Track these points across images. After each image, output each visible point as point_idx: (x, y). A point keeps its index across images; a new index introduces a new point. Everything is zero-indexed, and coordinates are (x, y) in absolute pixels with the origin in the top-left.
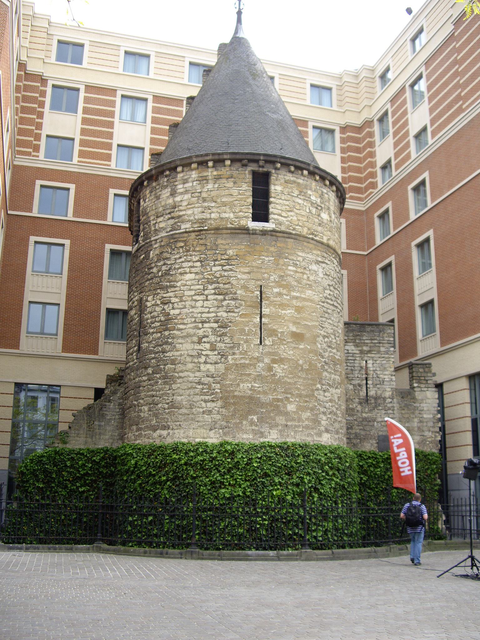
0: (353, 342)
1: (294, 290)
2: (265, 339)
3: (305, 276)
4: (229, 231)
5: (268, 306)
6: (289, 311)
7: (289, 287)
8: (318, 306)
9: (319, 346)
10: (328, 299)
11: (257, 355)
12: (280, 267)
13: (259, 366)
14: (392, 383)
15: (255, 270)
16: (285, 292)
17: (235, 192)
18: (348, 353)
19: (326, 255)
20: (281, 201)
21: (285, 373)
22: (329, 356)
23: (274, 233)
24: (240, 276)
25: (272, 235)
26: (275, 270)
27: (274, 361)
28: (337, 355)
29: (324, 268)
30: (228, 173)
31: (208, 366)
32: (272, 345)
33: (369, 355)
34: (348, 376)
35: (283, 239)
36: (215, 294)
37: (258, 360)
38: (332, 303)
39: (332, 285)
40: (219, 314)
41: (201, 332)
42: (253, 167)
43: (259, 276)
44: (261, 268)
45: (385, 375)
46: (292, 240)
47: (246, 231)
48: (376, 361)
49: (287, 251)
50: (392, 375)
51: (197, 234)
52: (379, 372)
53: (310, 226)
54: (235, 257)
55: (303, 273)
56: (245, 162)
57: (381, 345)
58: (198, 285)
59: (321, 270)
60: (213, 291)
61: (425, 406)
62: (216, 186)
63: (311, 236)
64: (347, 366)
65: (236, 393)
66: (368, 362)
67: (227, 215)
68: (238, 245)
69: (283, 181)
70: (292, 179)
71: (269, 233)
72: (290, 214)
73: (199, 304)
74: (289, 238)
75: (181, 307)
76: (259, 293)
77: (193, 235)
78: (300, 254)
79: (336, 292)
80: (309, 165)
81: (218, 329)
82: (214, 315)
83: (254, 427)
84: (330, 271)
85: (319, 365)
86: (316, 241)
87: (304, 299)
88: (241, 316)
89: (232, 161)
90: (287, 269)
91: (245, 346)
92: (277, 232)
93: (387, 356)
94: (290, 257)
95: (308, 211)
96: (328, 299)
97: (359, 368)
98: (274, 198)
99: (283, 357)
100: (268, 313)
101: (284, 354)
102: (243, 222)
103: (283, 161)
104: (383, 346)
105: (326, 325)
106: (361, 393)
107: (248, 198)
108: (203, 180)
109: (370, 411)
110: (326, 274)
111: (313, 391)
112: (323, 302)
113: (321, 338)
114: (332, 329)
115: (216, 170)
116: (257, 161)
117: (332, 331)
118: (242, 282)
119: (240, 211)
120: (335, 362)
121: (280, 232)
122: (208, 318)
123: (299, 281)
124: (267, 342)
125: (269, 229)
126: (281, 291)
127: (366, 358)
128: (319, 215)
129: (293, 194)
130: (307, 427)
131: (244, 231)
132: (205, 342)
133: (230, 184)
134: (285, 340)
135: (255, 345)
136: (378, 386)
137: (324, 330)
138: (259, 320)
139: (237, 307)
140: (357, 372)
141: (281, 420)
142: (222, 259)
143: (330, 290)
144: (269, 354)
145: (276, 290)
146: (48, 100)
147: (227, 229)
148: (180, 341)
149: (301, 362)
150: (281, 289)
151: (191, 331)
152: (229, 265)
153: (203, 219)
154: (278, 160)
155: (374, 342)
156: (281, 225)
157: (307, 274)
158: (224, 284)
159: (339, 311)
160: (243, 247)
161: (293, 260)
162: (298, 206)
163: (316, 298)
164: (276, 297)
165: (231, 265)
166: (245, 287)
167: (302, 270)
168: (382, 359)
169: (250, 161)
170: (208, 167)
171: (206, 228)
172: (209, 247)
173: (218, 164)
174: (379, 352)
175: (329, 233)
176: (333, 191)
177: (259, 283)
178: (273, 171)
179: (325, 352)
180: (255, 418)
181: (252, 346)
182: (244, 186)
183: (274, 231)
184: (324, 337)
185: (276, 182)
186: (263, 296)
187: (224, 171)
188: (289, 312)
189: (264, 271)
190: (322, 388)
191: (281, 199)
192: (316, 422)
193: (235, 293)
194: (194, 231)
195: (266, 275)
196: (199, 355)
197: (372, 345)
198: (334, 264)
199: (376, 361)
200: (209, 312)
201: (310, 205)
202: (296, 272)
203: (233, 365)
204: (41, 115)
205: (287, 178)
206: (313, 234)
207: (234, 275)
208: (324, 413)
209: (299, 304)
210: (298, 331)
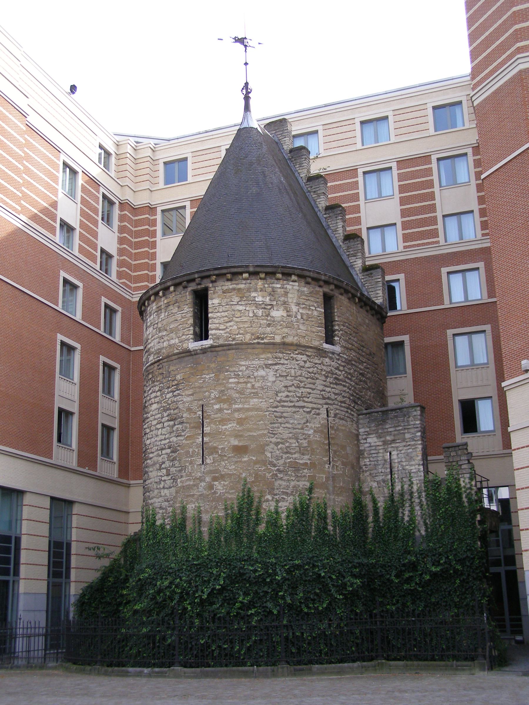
0: (376, 433)
1: (235, 403)
2: (206, 458)
3: (249, 385)
4: (176, 357)
5: (209, 423)
6: (230, 425)
7: (230, 401)
8: (267, 413)
9: (269, 455)
10: (284, 401)
11: (200, 475)
12: (220, 381)
13: (201, 486)
15: (197, 390)
16: (226, 406)
17: (179, 316)
18: (370, 446)
19: (281, 355)
20: (219, 314)
21: (226, 489)
22: (285, 463)
23: (213, 349)
24: (186, 399)
25: (212, 351)
26: (215, 386)
27: (215, 479)
29: (277, 370)
30: (174, 299)
31: (166, 491)
32: (212, 463)
33: (393, 445)
34: (372, 472)
35: (224, 352)
36: (168, 421)
37: (201, 479)
38: (292, 404)
39: (293, 385)
40: (171, 440)
41: (160, 459)
42: (193, 286)
44: (203, 387)
45: (412, 465)
46: (234, 351)
47: (188, 353)
48: (400, 451)
49: (228, 363)
51: (158, 364)
52: (404, 464)
53: (255, 330)
54: (182, 381)
55: (246, 383)
57: (406, 431)
58: (159, 414)
59: (272, 373)
60: (167, 418)
62: (166, 314)
63: (255, 341)
64: (370, 461)
66: (393, 453)
67: (173, 342)
68: (184, 368)
69: (220, 293)
70: (231, 287)
71: (209, 350)
72: (228, 324)
73: (160, 432)
74: (229, 350)
75: (151, 436)
76: (200, 413)
77: (156, 365)
78: (243, 363)
79: (303, 390)
80: (247, 266)
81: (171, 455)
82: (168, 441)
84: (288, 370)
85: (268, 475)
86: (264, 343)
87: (248, 410)
88: (186, 439)
89: (176, 285)
90: (228, 382)
91: (190, 468)
93: (413, 443)
94: (231, 369)
95: (251, 315)
96: (284, 401)
97: (383, 462)
98: (212, 313)
99: (223, 473)
100: (209, 432)
101: (225, 470)
102: (185, 346)
103: (216, 272)
104: (408, 433)
105: (280, 430)
107: (188, 320)
108: (159, 309)
110: (281, 376)
113: (272, 446)
114: (290, 433)
115: (166, 298)
116: (193, 280)
117: (290, 435)
118: (187, 405)
119: (183, 335)
120: (296, 467)
121: (219, 346)
122: (164, 445)
123: (241, 392)
124: (208, 461)
125: (207, 346)
126: (222, 407)
127: (390, 449)
128: (268, 315)
129: (232, 303)
131: (187, 354)
132: (163, 468)
133: (175, 310)
134: (225, 456)
135: (197, 465)
137: (276, 436)
138: (201, 440)
139: (183, 431)
140: (380, 467)
142: (173, 386)
143: (289, 392)
144: (211, 472)
145: (217, 407)
146: (159, 228)
148: (151, 469)
149: (244, 475)
150: (222, 404)
151: (155, 459)
152: (178, 390)
153: (159, 349)
154: (212, 273)
155: (398, 429)
156: (218, 339)
157: (251, 382)
158: (174, 409)
159: (308, 410)
160: (188, 369)
161: (235, 371)
162: (239, 313)
163: (264, 405)
164: (217, 414)
165: (180, 389)
166: (189, 410)
167: (245, 380)
168: (408, 447)
169: (189, 281)
170: (161, 297)
171: (161, 357)
172: (164, 376)
173: (167, 292)
174: (404, 440)
175: (286, 330)
176: (294, 281)
177: (201, 403)
178: (211, 285)
179: (278, 460)
181: (195, 466)
182: (186, 308)
183: (212, 347)
184: (277, 444)
185: (214, 296)
186: (205, 415)
187: (172, 297)
188: (230, 426)
189: (205, 389)
190: (273, 498)
191: (218, 312)
193: (182, 417)
194: (155, 362)
195: (207, 393)
196: (159, 483)
197: (396, 433)
198: (297, 361)
199: (400, 451)
200: (165, 439)
201: (254, 308)
202: (238, 383)
203: (181, 487)
204: (154, 245)
205: (225, 288)
206: (258, 338)
207: (180, 399)
209: (242, 416)
210: (241, 444)
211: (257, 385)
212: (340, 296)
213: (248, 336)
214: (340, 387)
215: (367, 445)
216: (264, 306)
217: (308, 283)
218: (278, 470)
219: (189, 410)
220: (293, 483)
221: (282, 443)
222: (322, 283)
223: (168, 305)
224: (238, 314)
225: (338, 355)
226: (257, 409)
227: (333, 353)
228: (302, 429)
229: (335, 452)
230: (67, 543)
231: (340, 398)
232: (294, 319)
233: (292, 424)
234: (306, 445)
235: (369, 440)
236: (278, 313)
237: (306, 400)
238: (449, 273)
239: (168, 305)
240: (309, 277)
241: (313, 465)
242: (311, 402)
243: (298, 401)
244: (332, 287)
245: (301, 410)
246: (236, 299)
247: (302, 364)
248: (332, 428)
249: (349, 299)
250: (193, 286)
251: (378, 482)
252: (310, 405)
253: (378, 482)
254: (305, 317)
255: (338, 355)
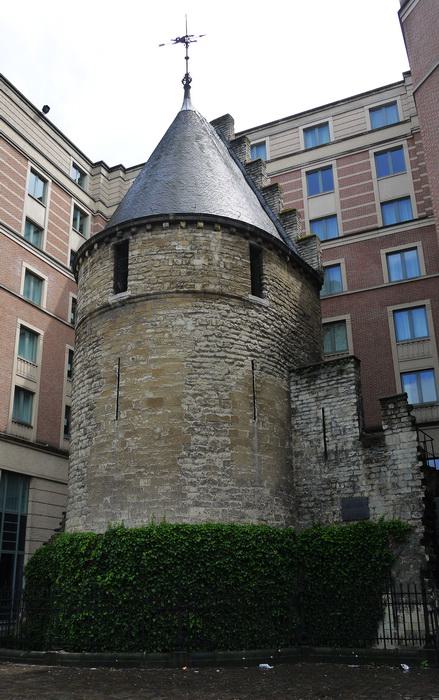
5: (124, 377)
7: (146, 352)
9: (186, 407)
10: (204, 351)
14: (354, 430)
19: (201, 304)
22: (203, 416)
23: (132, 301)
27: (128, 435)
28: (223, 413)
31: (83, 451)
33: (326, 401)
38: (212, 354)
42: (115, 241)
43: (117, 349)
47: (107, 308)
50: (354, 420)
52: (337, 420)
56: (107, 239)
59: (190, 322)
61: (398, 453)
65: (97, 475)
66: (326, 410)
67: (95, 298)
72: (148, 274)
80: (167, 215)
83: (107, 510)
85: (184, 430)
87: (164, 360)
89: (100, 242)
92: (134, 298)
96: (204, 351)
102: (105, 300)
106: (319, 450)
109: (330, 470)
111: (174, 460)
112: (195, 357)
113: (189, 398)
116: (114, 234)
120: (215, 421)
121: (137, 297)
124: (122, 416)
130: (165, 503)
136: (338, 437)
141: (131, 498)
147: (95, 311)
149: (158, 430)
163: (181, 355)
166: (106, 364)
174: (337, 395)
177: (118, 356)
180: (108, 499)
183: (130, 298)
184: (195, 396)
187: (96, 255)
192: (180, 494)
202: (156, 333)
208: (192, 483)
209: (158, 367)
210: (156, 397)
211: (175, 335)
212: (269, 251)
213: (167, 285)
214: (266, 340)
215: (298, 403)
216: (184, 255)
217: (232, 233)
218: (196, 424)
219: (106, 364)
220: (211, 439)
221: (200, 395)
222: (248, 234)
223: (93, 263)
224: (158, 264)
225: (266, 308)
226: (173, 360)
227: (260, 306)
228: (223, 380)
229: (261, 406)
230: (22, 517)
231: (267, 351)
232: (217, 268)
233: (211, 374)
234: (227, 397)
235: (300, 398)
236: (198, 262)
237: (228, 350)
238: (388, 254)
239: (93, 263)
240: (233, 227)
241: (234, 420)
242: (234, 353)
243: (219, 351)
244: (259, 240)
245: (223, 360)
246: (156, 248)
247: (225, 313)
248: (258, 381)
249: (279, 255)
250: (115, 241)
251: (311, 442)
252: (233, 356)
253: (311, 442)
254: (228, 267)
255: (266, 308)
